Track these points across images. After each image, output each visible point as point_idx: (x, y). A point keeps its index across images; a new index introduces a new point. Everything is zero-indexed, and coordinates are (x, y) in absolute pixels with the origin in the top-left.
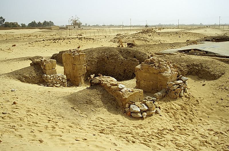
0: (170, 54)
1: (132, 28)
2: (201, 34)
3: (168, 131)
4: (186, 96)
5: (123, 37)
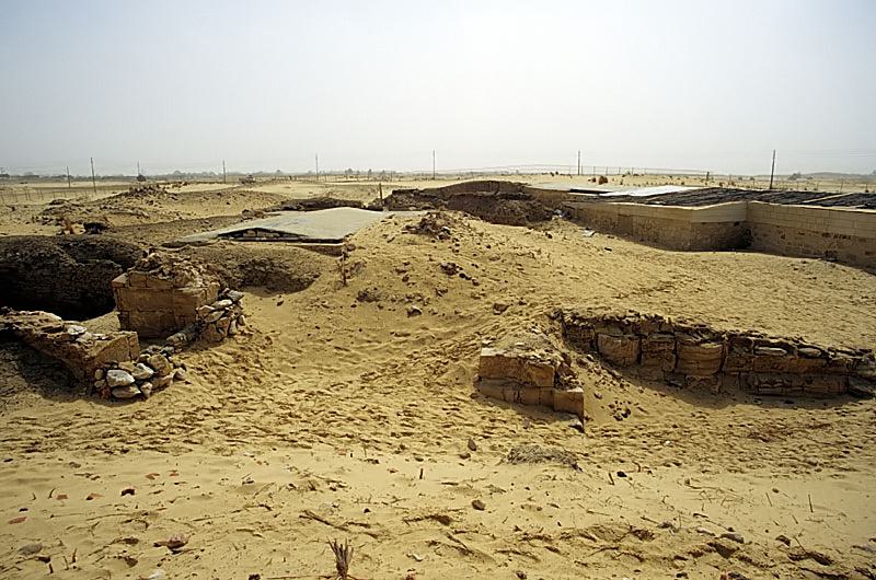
0: (200, 244)
1: (97, 184)
2: (277, 195)
3: (207, 412)
4: (243, 333)
5: (71, 208)
